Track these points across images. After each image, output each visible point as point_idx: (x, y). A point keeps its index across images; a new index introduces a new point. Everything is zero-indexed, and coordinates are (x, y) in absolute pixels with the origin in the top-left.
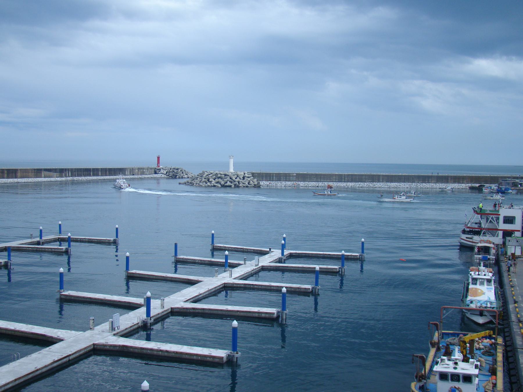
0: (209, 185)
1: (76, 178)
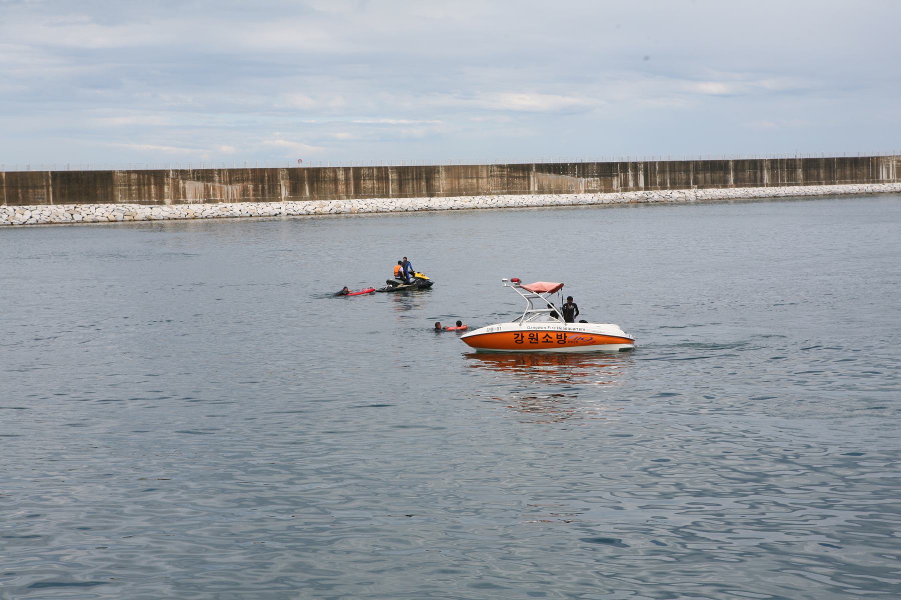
1: (656, 195)
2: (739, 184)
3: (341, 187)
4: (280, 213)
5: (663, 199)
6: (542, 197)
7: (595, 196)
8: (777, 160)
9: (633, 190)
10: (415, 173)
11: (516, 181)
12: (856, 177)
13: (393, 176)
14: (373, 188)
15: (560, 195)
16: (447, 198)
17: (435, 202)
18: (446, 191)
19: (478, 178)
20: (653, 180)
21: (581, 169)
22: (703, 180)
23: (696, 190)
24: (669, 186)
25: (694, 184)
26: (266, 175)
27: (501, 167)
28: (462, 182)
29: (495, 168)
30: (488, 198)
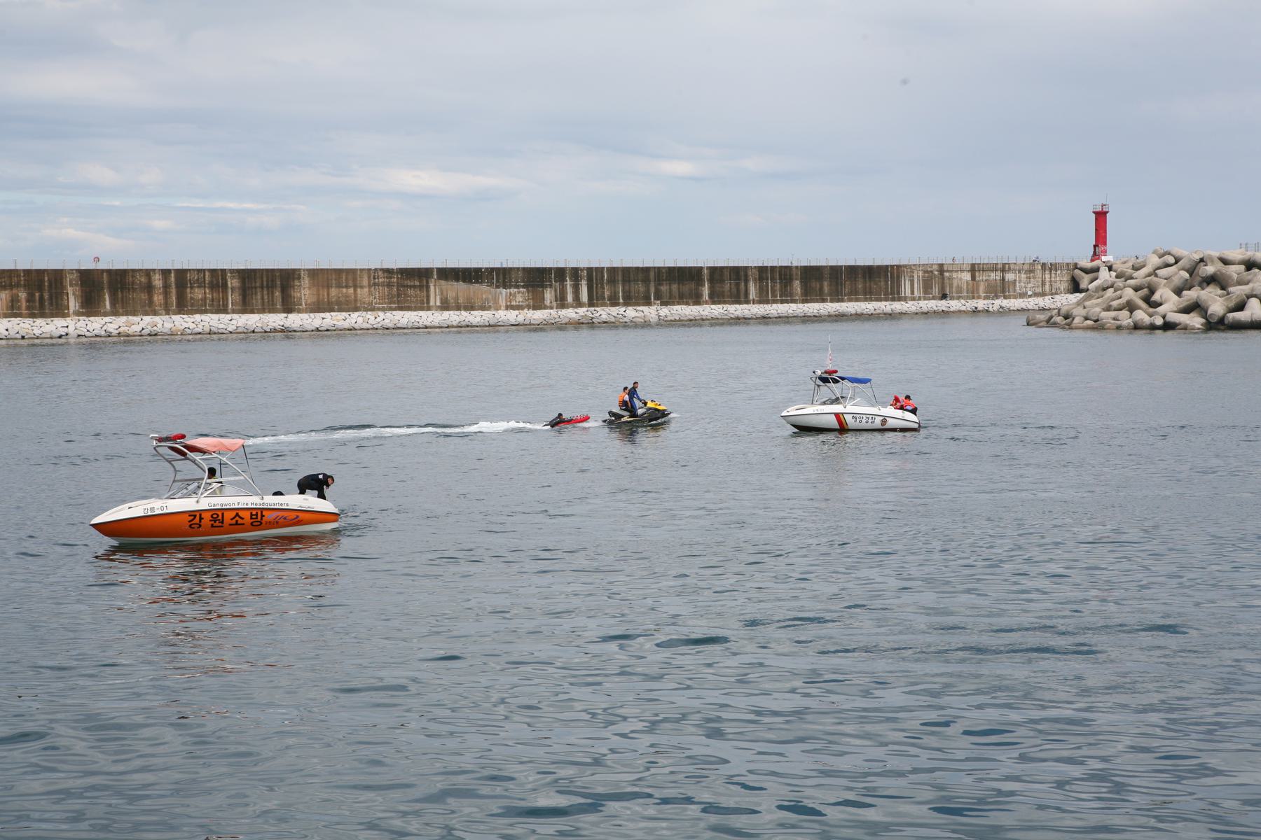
0: (1140, 323)
2: (716, 299)
3: (158, 298)
4: (67, 334)
5: (613, 320)
6: (446, 314)
7: (520, 314)
8: (767, 267)
9: (572, 307)
10: (265, 279)
11: (410, 292)
12: (871, 293)
13: (233, 283)
14: (204, 299)
15: (472, 312)
16: (311, 314)
17: (295, 320)
18: (310, 305)
19: (355, 287)
20: (599, 293)
21: (501, 276)
22: (668, 294)
23: (659, 308)
24: (621, 301)
25: (655, 299)
26: (46, 279)
27: (389, 272)
28: (334, 292)
29: (380, 273)
30: (370, 315)
